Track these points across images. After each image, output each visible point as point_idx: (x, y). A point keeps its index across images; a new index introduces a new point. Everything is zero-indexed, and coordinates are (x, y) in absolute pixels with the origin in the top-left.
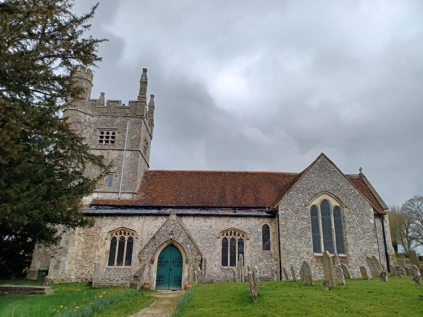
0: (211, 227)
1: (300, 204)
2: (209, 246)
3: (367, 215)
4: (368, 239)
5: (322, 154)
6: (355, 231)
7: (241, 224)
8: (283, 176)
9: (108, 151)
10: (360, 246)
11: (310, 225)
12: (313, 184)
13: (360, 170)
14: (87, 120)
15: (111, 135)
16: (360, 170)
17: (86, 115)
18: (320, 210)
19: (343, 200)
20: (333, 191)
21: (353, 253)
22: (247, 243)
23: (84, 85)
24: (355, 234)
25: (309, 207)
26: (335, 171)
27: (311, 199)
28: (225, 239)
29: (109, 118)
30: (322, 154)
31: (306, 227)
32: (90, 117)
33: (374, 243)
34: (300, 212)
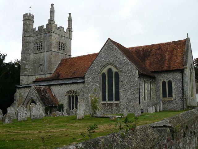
5: (109, 39)
14: (31, 40)
15: (41, 45)
17: (31, 38)
18: (107, 76)
22: (78, 97)
25: (101, 74)
29: (40, 36)
30: (109, 39)
33: (136, 93)
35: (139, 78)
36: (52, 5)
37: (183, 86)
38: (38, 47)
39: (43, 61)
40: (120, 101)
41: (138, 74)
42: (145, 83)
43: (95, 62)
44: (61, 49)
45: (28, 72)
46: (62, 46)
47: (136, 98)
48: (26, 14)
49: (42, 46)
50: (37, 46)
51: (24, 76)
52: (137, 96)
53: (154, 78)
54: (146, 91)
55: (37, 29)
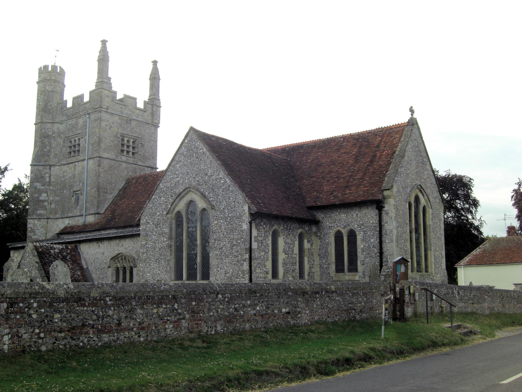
0: (103, 254)
1: (161, 212)
2: (102, 277)
3: (240, 217)
4: (236, 256)
5: (192, 129)
6: (220, 246)
7: (129, 247)
9: (74, 164)
10: (225, 267)
12: (178, 179)
13: (412, 111)
15: (77, 142)
16: (412, 111)
17: (54, 124)
19: (210, 198)
20: (199, 185)
21: (216, 279)
23: (47, 88)
24: (220, 249)
26: (203, 152)
28: (118, 268)
29: (74, 121)
30: (192, 129)
31: (165, 246)
32: (59, 125)
34: (161, 224)
35: (250, 223)
36: (104, 42)
37: (381, 243)
38: (70, 147)
39: (80, 182)
40: (211, 279)
41: (247, 213)
42: (275, 237)
43: (161, 185)
44: (128, 152)
45: (46, 209)
46: (131, 144)
47: (243, 271)
48: (46, 67)
49: (79, 145)
50: (69, 144)
51: (36, 221)
52: (246, 266)
53: (316, 222)
54: (281, 256)
55: (69, 105)
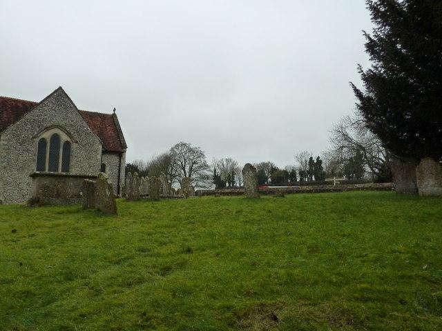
3: (96, 151)
5: (60, 88)
8: (24, 103)
11: (36, 158)
13: (115, 110)
16: (115, 110)
18: (49, 144)
25: (37, 140)
27: (41, 131)
30: (60, 88)
